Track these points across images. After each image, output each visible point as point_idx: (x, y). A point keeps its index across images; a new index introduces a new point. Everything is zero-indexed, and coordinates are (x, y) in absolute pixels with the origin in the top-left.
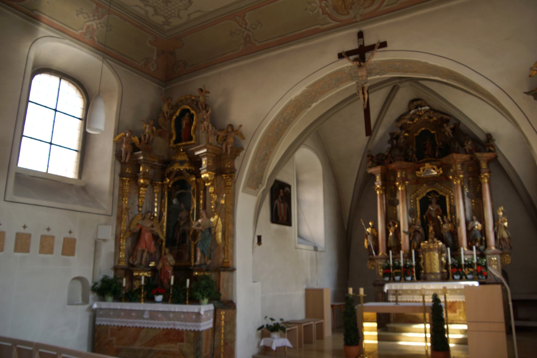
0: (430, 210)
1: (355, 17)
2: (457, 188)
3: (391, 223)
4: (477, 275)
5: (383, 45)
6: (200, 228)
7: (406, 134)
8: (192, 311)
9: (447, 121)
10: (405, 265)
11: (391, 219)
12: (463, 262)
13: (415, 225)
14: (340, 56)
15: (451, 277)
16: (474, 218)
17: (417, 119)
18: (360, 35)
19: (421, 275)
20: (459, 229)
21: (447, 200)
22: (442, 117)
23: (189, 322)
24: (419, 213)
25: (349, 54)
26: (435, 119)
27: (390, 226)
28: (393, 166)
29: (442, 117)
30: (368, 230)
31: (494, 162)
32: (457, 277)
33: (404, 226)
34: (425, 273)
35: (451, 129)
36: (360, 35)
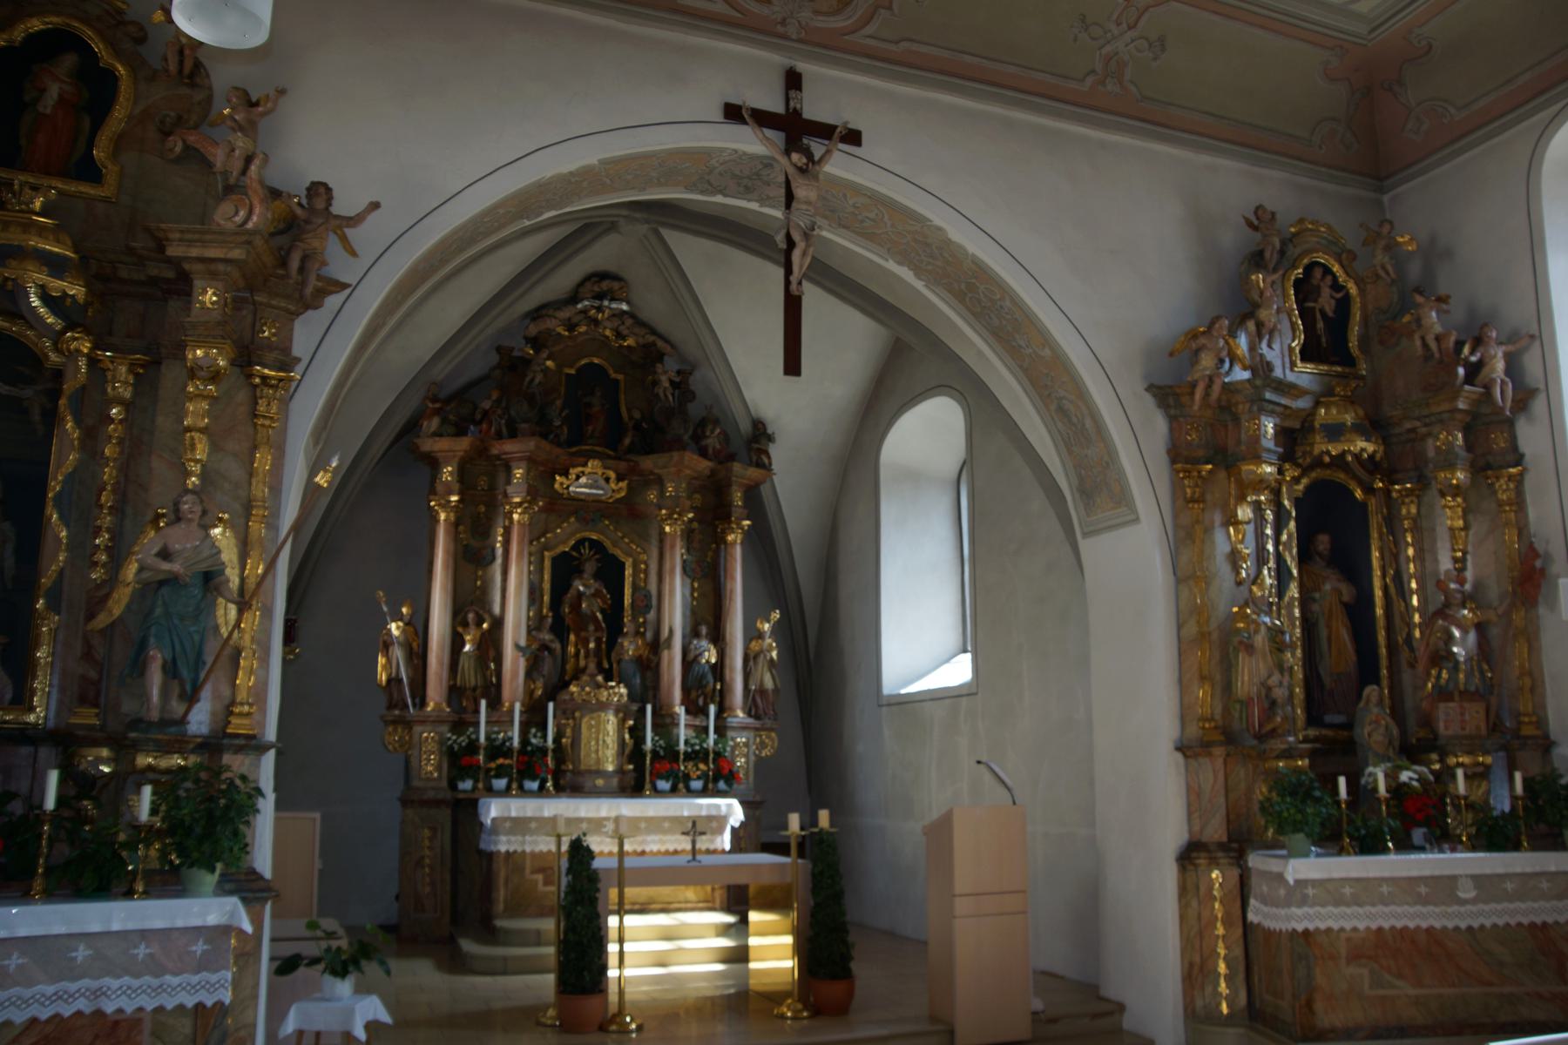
0: (580, 595)
1: (783, 22)
2: (673, 547)
3: (471, 616)
4: (716, 780)
5: (853, 137)
6: (175, 567)
7: (549, 363)
8: (196, 922)
9: (660, 357)
10: (525, 741)
11: (470, 603)
12: (682, 747)
13: (539, 628)
14: (733, 113)
15: (648, 786)
16: (704, 630)
17: (583, 329)
18: (793, 80)
19: (568, 778)
20: (665, 653)
21: (628, 572)
22: (654, 344)
23: (175, 974)
24: (546, 598)
25: (762, 119)
26: (630, 342)
27: (466, 625)
28: (510, 447)
29: (654, 344)
30: (393, 626)
31: (753, 495)
32: (663, 785)
33: (514, 632)
34: (577, 772)
35: (672, 382)
36: (793, 80)
